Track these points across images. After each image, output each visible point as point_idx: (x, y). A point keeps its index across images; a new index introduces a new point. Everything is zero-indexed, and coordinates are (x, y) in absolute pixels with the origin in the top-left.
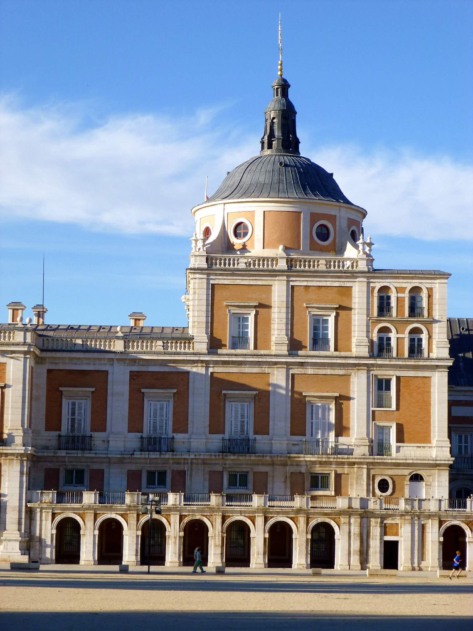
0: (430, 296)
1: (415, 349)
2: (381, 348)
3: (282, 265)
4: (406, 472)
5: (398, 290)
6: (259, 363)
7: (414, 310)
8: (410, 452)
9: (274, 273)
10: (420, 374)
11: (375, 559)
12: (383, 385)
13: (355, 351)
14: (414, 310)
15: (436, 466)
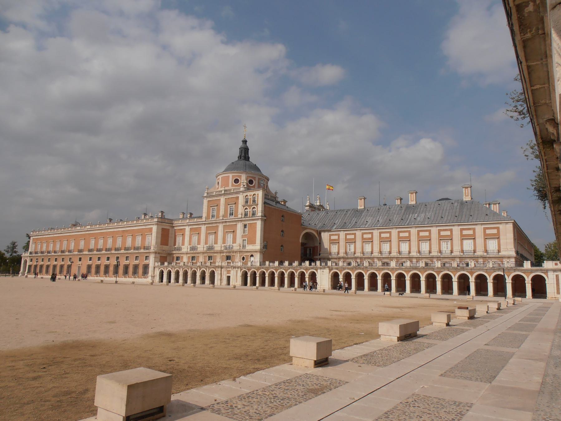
0: (258, 196)
1: (254, 214)
2: (246, 215)
3: (223, 192)
4: (249, 254)
5: (250, 195)
6: (216, 223)
7: (254, 201)
8: (249, 247)
9: (220, 195)
10: (254, 222)
11: (225, 282)
12: (245, 226)
13: (240, 216)
14: (254, 201)
15: (256, 251)
